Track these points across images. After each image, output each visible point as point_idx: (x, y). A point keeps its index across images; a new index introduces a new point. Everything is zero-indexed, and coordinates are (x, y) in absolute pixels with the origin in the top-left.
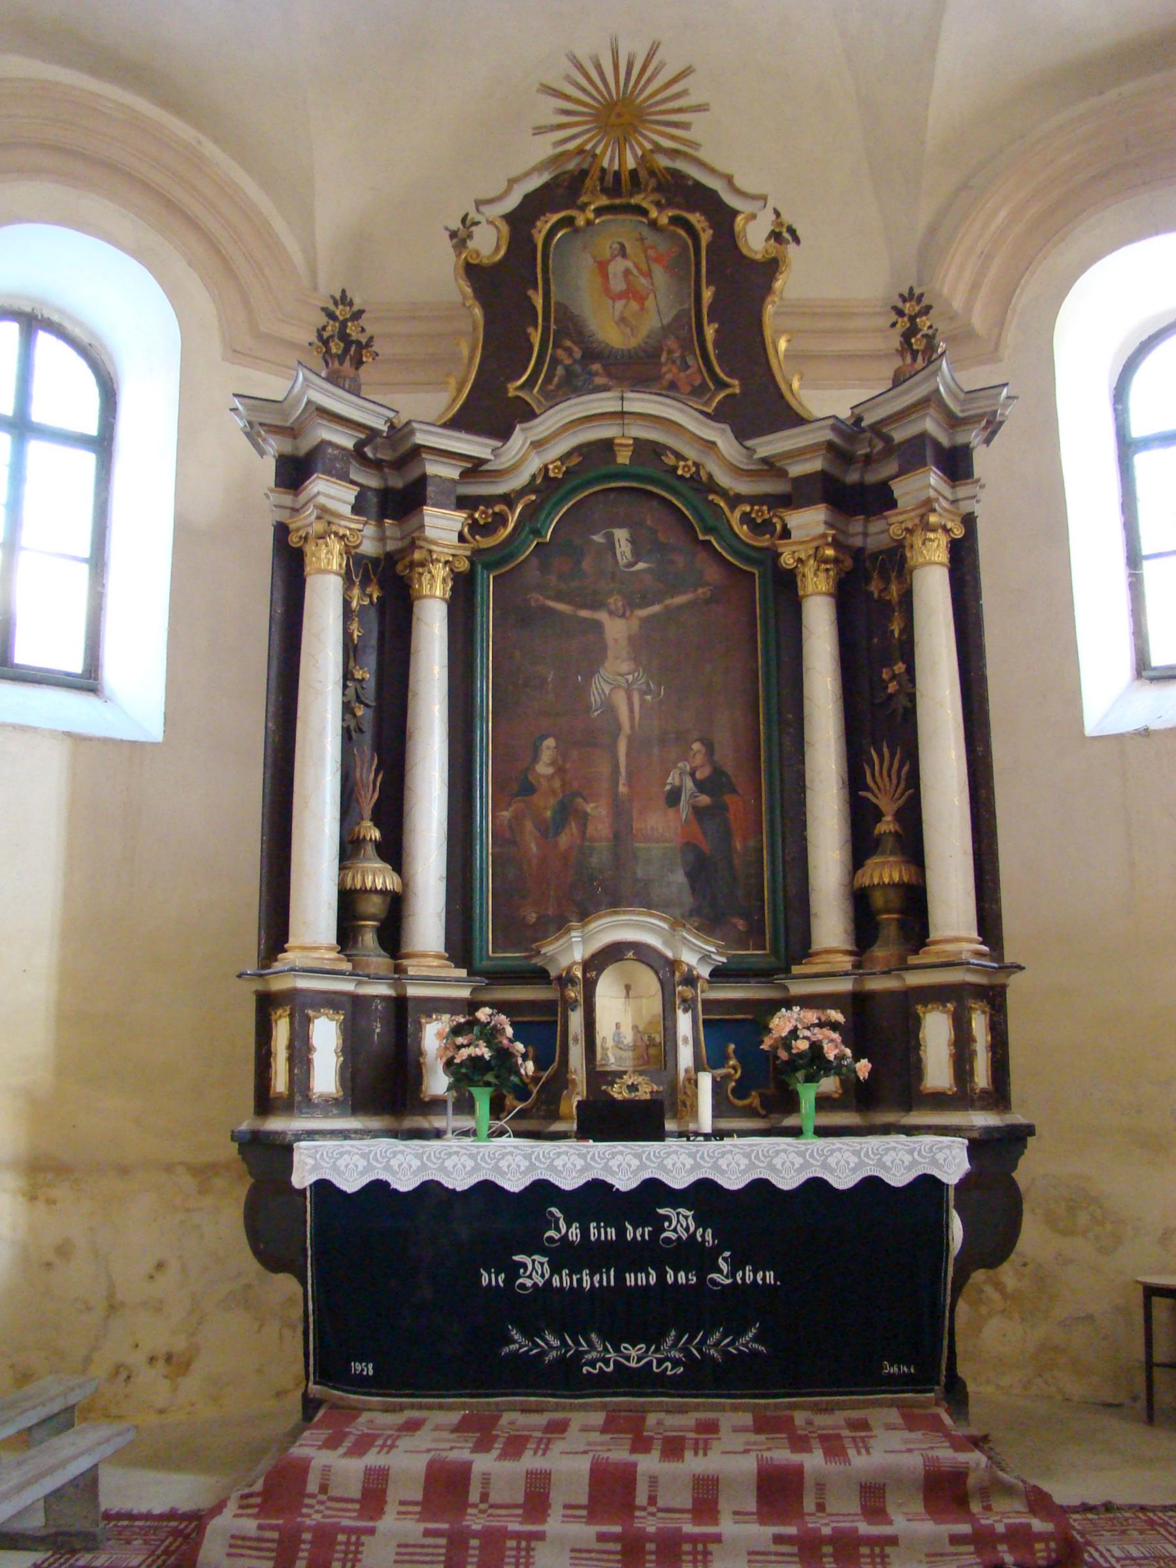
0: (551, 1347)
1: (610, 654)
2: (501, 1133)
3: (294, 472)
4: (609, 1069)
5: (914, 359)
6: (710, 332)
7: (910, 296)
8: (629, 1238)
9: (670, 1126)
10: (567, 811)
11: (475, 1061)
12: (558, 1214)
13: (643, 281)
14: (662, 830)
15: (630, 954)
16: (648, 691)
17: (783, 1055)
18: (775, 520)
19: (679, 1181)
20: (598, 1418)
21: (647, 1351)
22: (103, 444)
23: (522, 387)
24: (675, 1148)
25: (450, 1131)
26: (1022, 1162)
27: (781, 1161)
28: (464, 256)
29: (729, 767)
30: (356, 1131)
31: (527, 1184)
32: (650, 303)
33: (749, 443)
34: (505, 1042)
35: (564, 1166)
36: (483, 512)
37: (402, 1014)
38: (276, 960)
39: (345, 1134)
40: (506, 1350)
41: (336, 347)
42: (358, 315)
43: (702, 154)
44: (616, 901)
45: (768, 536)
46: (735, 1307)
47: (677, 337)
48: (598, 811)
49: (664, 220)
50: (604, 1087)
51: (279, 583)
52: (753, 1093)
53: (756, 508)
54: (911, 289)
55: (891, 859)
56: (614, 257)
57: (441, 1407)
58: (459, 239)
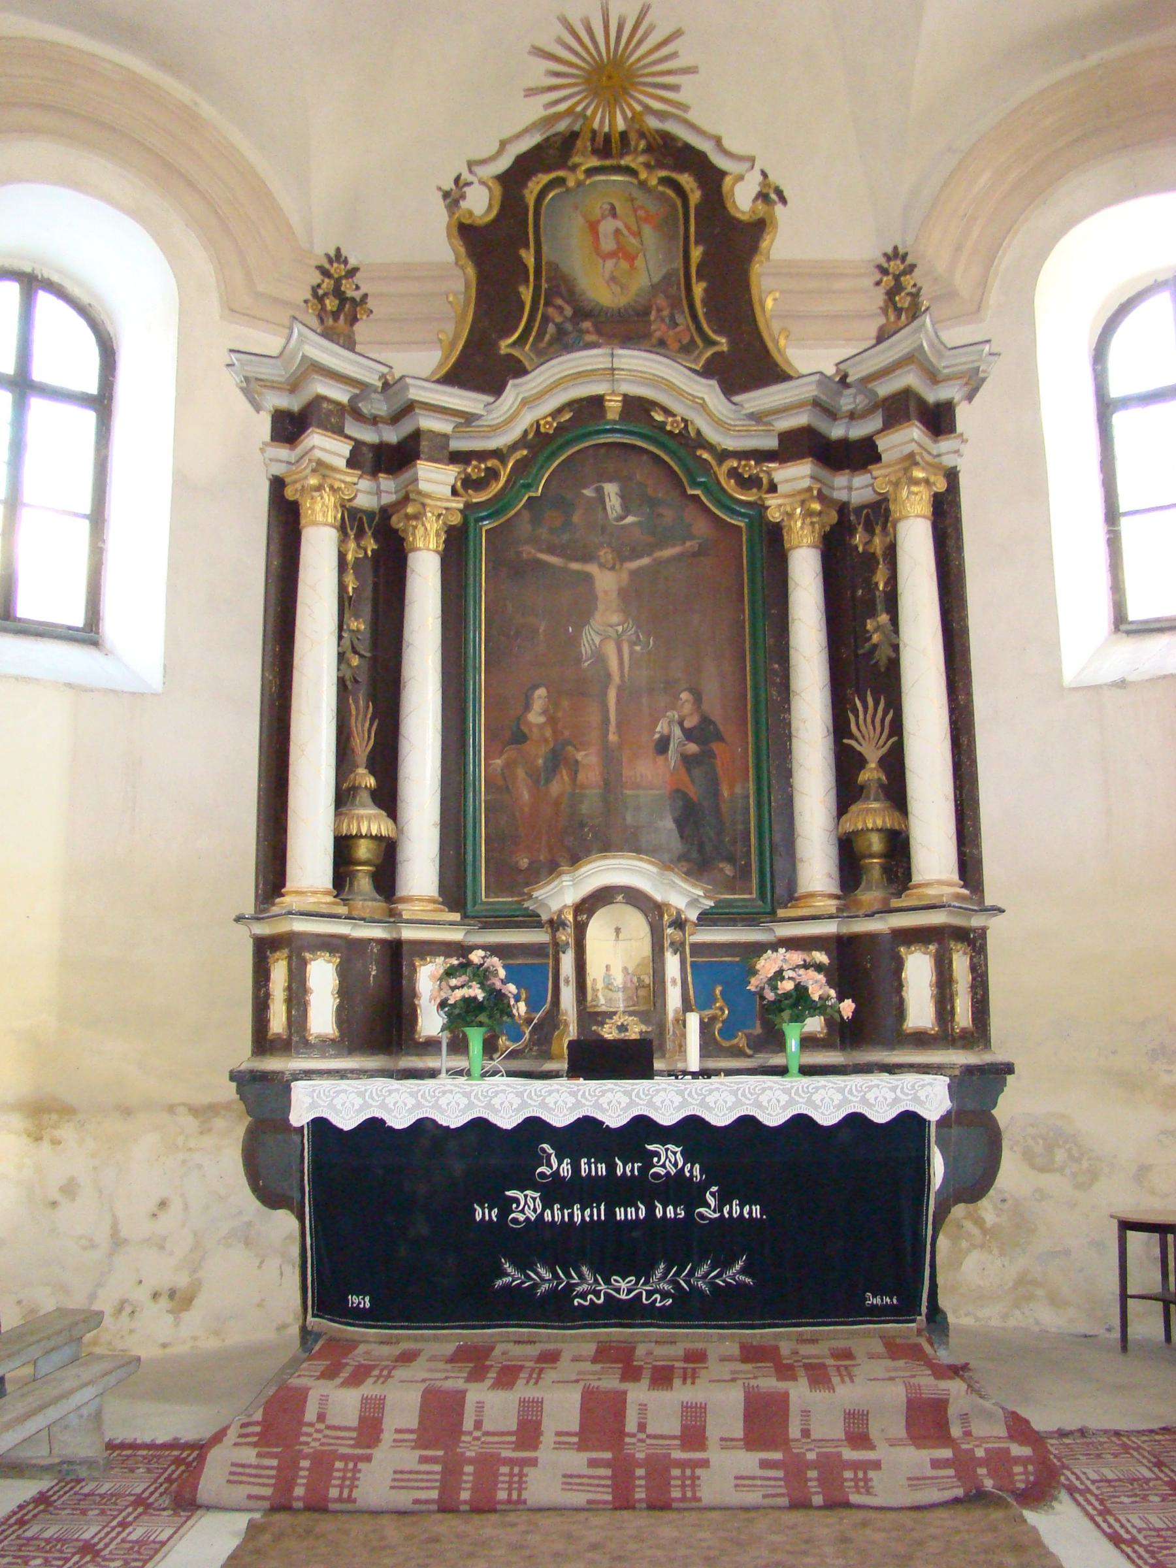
1: (601, 607)
2: (494, 1073)
3: (289, 427)
4: (599, 1010)
5: (899, 317)
6: (699, 289)
7: (895, 255)
8: (619, 1174)
9: (658, 1065)
10: (558, 759)
11: (469, 1002)
12: (550, 1151)
13: (633, 241)
14: (652, 777)
15: (620, 898)
16: (638, 641)
17: (770, 996)
18: (761, 475)
19: (667, 1118)
20: (590, 1349)
21: (637, 1283)
22: (102, 403)
23: (514, 344)
24: (664, 1086)
25: (444, 1071)
26: (1001, 1099)
28: (456, 216)
29: (716, 715)
30: (352, 1071)
32: (639, 262)
33: (736, 399)
36: (475, 467)
37: (396, 958)
38: (273, 904)
39: (341, 1074)
40: (499, 1283)
41: (331, 304)
42: (353, 272)
43: (691, 116)
44: (607, 847)
45: (755, 490)
46: (722, 1241)
47: (667, 297)
48: (588, 758)
49: (653, 182)
50: (594, 1028)
51: (275, 536)
53: (743, 463)
54: (896, 248)
55: (875, 805)
56: (603, 217)
57: (436, 1338)
58: (453, 198)
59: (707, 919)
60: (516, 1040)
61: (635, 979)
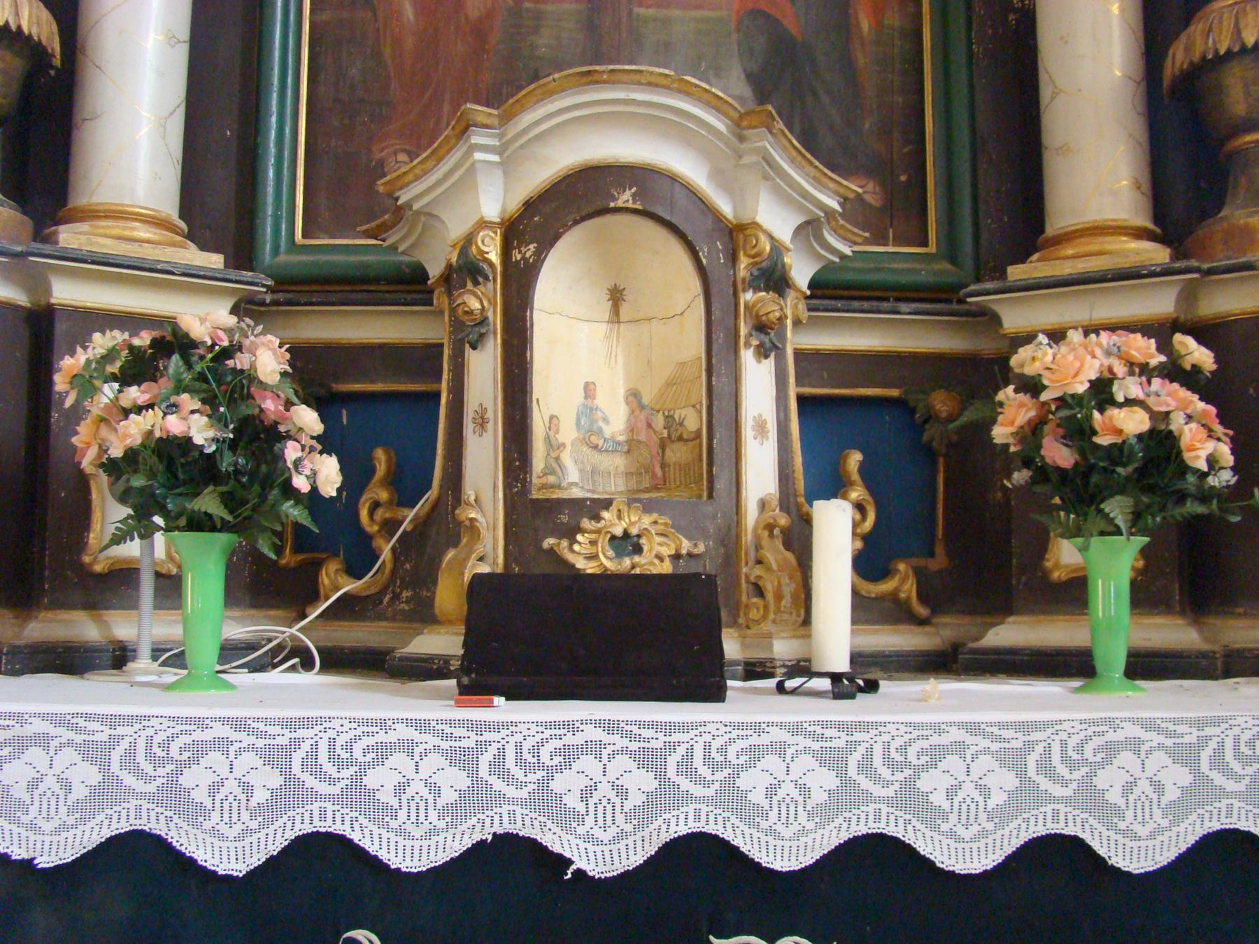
9: (732, 647)
11: (171, 453)
25: (145, 650)
27: (1121, 779)
31: (275, 848)
34: (270, 406)
35: (400, 789)
50: (549, 542)
52: (902, 567)
59: (830, 291)
60: (355, 571)
61: (659, 422)
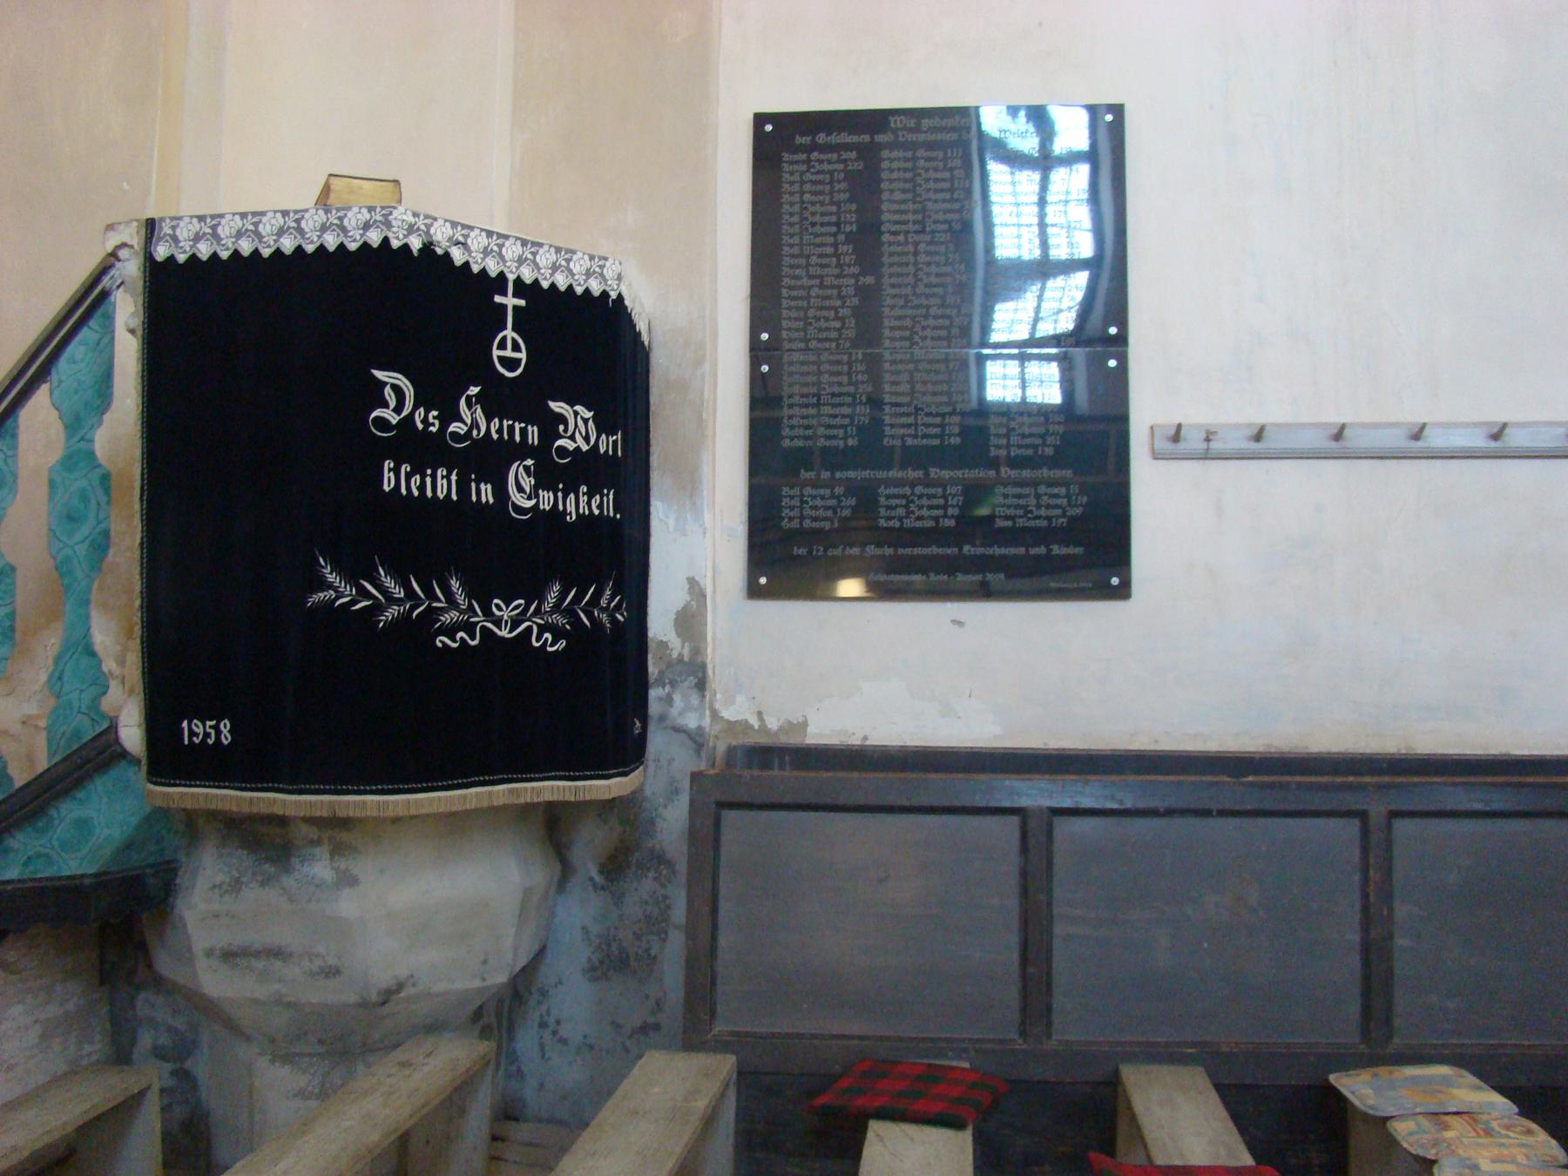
0: (391, 600)
